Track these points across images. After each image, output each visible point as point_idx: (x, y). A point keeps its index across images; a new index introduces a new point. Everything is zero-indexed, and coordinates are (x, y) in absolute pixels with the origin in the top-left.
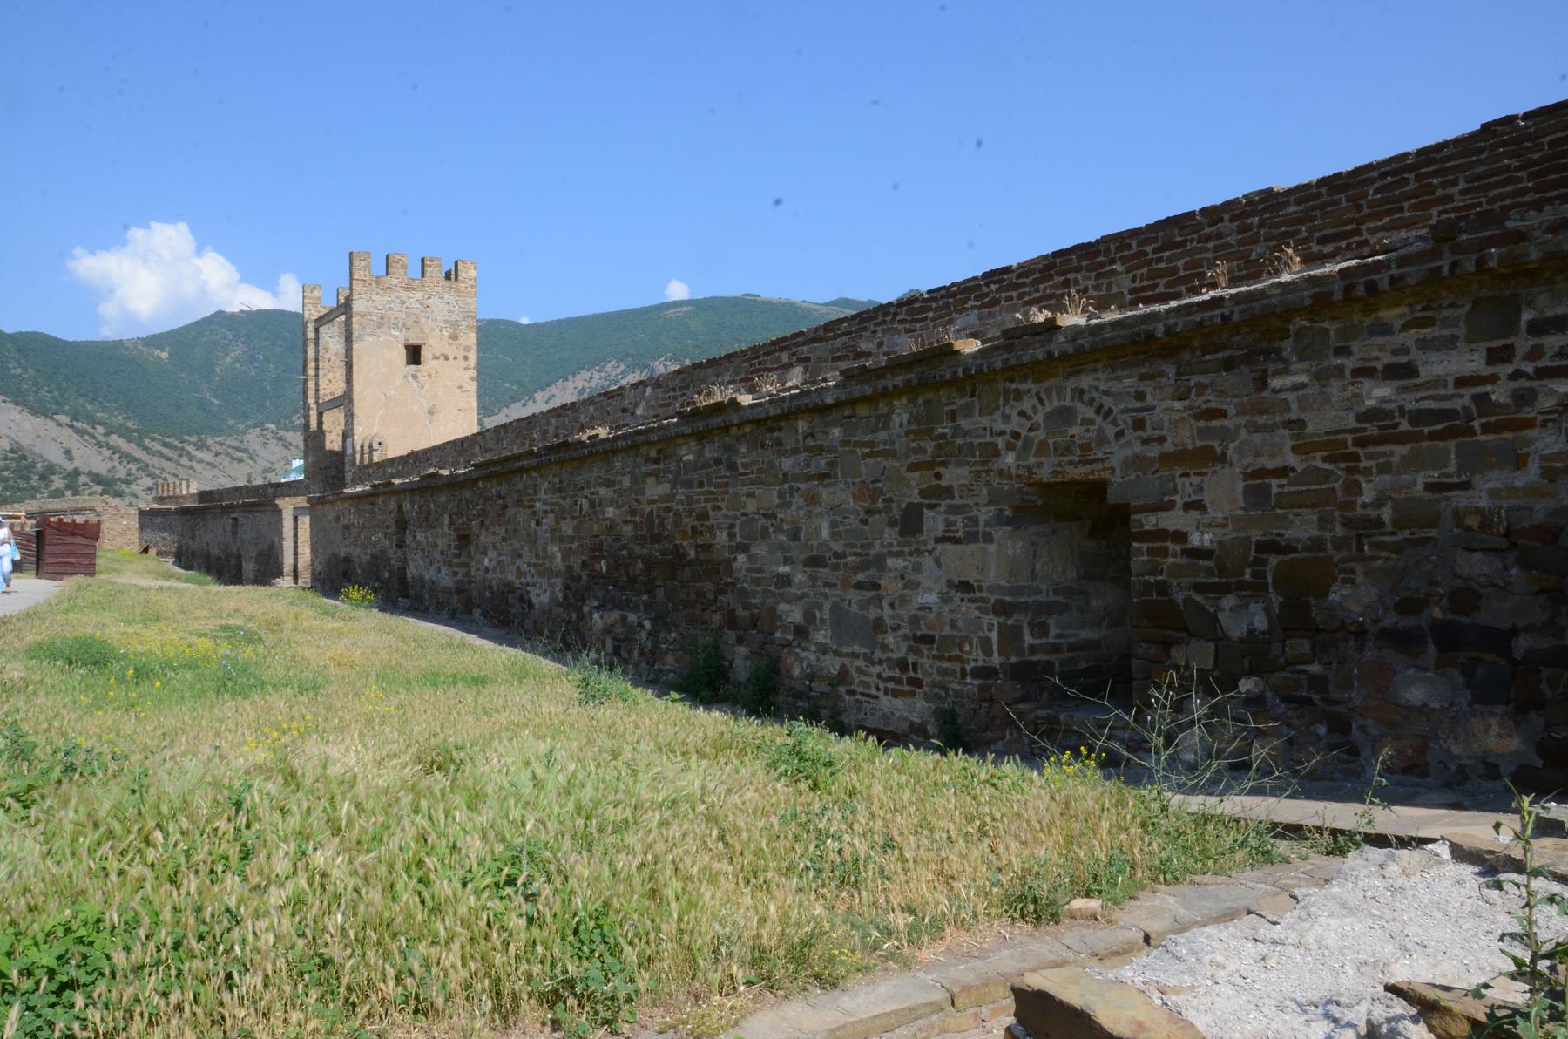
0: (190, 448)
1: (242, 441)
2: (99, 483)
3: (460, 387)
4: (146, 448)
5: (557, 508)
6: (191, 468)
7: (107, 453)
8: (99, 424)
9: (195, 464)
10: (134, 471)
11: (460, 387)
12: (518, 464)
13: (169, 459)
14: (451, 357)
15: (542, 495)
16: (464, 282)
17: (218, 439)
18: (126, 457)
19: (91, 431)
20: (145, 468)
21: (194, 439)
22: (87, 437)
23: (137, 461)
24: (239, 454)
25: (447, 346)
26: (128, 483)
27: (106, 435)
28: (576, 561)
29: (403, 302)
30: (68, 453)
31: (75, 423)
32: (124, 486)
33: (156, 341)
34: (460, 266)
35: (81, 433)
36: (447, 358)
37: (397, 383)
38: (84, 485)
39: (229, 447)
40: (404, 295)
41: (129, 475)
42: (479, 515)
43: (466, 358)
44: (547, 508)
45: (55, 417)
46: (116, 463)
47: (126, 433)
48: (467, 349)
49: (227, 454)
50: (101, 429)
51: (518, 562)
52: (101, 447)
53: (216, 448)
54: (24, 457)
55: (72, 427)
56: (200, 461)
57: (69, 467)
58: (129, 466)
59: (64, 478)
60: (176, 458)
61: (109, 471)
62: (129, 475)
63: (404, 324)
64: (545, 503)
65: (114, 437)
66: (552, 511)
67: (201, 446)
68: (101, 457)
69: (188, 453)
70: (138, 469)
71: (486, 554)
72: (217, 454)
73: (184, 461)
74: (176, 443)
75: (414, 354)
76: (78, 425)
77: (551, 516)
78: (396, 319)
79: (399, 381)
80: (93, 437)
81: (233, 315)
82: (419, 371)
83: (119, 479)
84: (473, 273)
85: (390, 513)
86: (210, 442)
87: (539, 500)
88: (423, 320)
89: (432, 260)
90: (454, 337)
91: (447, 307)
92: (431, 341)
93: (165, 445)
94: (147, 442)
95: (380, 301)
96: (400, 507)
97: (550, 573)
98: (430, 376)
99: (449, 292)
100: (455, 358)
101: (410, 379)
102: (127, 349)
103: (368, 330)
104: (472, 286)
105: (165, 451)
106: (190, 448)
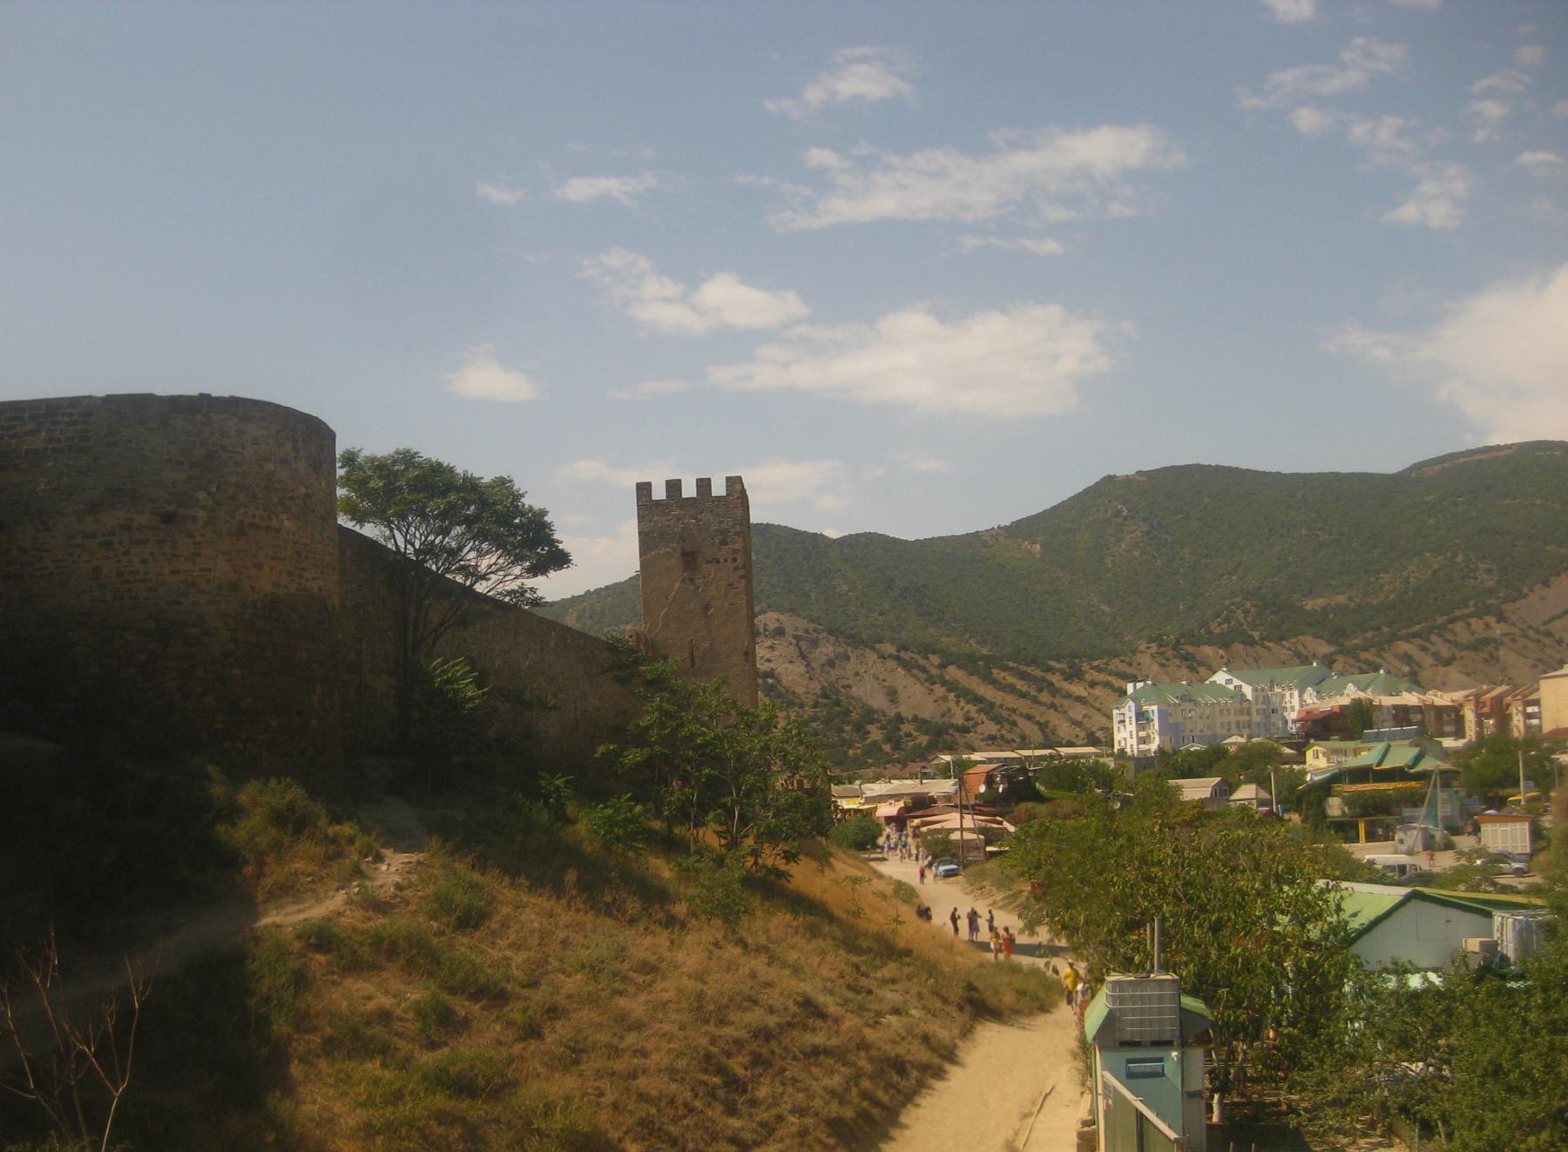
4: (994, 682)
7: (940, 690)
8: (934, 652)
9: (1057, 701)
10: (974, 714)
17: (1096, 663)
19: (922, 662)
20: (988, 708)
22: (915, 671)
23: (978, 700)
26: (965, 730)
27: (943, 666)
30: (892, 694)
31: (902, 654)
32: (957, 735)
33: (1023, 529)
35: (907, 666)
36: (718, 562)
38: (908, 735)
41: (968, 719)
43: (735, 560)
45: (878, 646)
46: (952, 704)
47: (969, 663)
48: (736, 551)
49: (1107, 685)
50: (935, 660)
52: (934, 683)
53: (1092, 675)
54: (838, 703)
55: (898, 658)
56: (1069, 696)
57: (892, 711)
59: (881, 728)
60: (1033, 693)
61: (943, 716)
62: (968, 719)
67: (1074, 675)
68: (933, 698)
69: (1051, 684)
70: (979, 711)
72: (1093, 684)
73: (1045, 697)
74: (1038, 673)
80: (924, 670)
81: (1127, 481)
86: (1085, 666)
93: (1023, 676)
101: (687, 581)
102: (985, 545)
105: (1020, 685)
106: (1056, 679)
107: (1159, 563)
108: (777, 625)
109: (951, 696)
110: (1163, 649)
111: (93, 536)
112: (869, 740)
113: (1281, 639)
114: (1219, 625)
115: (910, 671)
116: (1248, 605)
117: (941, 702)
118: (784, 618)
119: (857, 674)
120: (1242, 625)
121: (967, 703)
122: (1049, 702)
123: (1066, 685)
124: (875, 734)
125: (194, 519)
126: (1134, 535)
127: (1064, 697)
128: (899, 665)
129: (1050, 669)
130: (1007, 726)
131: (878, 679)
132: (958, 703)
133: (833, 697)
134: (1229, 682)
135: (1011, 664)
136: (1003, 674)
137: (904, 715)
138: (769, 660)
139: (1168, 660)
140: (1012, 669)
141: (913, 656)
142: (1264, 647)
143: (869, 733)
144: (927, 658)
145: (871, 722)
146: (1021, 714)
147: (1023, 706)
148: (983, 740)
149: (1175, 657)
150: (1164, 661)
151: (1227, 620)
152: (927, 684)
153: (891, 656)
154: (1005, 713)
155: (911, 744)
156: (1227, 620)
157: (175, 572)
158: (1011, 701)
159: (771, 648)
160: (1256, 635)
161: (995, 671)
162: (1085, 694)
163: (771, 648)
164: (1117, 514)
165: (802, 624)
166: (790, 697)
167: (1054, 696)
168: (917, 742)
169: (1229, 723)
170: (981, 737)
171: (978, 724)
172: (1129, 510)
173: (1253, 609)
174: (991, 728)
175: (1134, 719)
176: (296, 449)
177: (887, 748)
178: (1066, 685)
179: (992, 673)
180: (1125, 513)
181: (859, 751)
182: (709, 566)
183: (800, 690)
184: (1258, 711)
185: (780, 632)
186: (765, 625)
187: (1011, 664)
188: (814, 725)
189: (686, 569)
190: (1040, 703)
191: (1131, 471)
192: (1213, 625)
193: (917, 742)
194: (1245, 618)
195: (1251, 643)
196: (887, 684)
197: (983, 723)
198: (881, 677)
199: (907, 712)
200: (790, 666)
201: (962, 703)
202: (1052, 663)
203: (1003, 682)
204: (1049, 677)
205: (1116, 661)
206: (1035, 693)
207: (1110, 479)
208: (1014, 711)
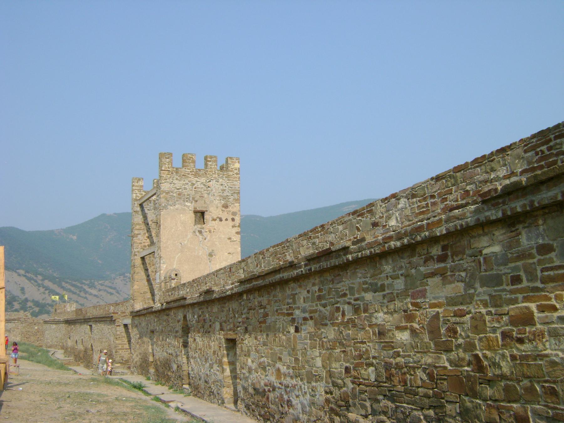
1: (113, 283)
2: (37, 306)
3: (230, 239)
4: (63, 287)
5: (316, 315)
6: (86, 298)
7: (42, 290)
8: (40, 274)
9: (87, 296)
11: (230, 239)
12: (278, 277)
14: (224, 219)
15: (301, 303)
16: (231, 171)
17: (100, 282)
19: (35, 278)
21: (87, 282)
22: (33, 282)
24: (111, 291)
25: (221, 213)
27: (43, 280)
28: (337, 367)
29: (193, 184)
31: (27, 274)
32: (50, 308)
33: (71, 230)
34: (229, 162)
35: (29, 279)
36: (221, 220)
37: (189, 236)
39: (106, 286)
40: (194, 180)
42: (243, 323)
43: (233, 220)
44: (307, 315)
45: (17, 271)
48: (234, 214)
49: (105, 290)
50: (40, 277)
51: (279, 365)
53: (99, 287)
55: (25, 276)
56: (91, 294)
57: (23, 297)
59: (19, 304)
60: (78, 293)
61: (43, 300)
63: (193, 199)
64: (304, 311)
66: (311, 318)
67: (92, 286)
69: (84, 290)
71: (249, 356)
72: (100, 290)
73: (82, 294)
74: (79, 284)
75: (201, 215)
76: (29, 275)
77: (311, 322)
78: (188, 195)
79: (190, 235)
80: (36, 281)
82: (203, 228)
83: (48, 304)
84: (237, 165)
85: (179, 321)
86: (96, 283)
87: (298, 308)
88: (206, 196)
89: (211, 157)
91: (221, 187)
92: (211, 209)
95: (178, 184)
96: (185, 317)
97: (311, 377)
98: (210, 231)
99: (222, 178)
100: (226, 220)
101: (198, 234)
103: (170, 203)
104: (237, 174)
105: (72, 289)
106: (86, 287)
109: (47, 292)
110: (125, 278)
115: (30, 281)
117: (42, 294)
123: (90, 290)
129: (82, 283)
131: (17, 284)
136: (66, 285)
137: (29, 299)
139: (127, 282)
140: (69, 283)
141: (31, 275)
143: (14, 305)
144: (37, 277)
145: (15, 301)
153: (23, 275)
161: (63, 283)
162: (97, 294)
168: (34, 310)
178: (90, 290)
182: (213, 222)
189: (196, 223)
190: (81, 297)
193: (34, 310)
196: (21, 286)
198: (18, 283)
199: (30, 298)
202: (84, 281)
205: (107, 282)
207: (103, 215)
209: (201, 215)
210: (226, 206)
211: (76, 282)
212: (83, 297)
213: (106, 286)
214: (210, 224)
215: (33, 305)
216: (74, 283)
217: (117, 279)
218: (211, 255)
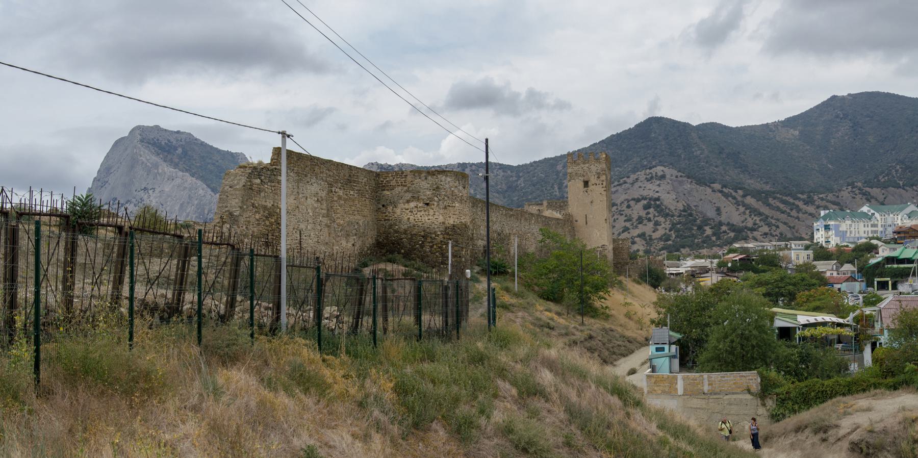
0: (800, 204)
1: (838, 197)
2: (733, 231)
4: (769, 205)
6: (798, 218)
7: (742, 209)
8: (740, 189)
9: (800, 215)
10: (758, 222)
13: (783, 212)
17: (821, 196)
18: (754, 212)
19: (734, 194)
20: (765, 219)
21: (805, 196)
22: (730, 199)
23: (760, 214)
27: (744, 196)
31: (724, 190)
32: (749, 232)
33: (790, 122)
35: (726, 196)
38: (725, 232)
39: (828, 201)
40: (583, 166)
41: (755, 224)
43: (602, 184)
45: (712, 185)
46: (747, 216)
47: (757, 194)
48: (603, 181)
50: (740, 192)
52: (739, 205)
54: (691, 215)
55: (721, 192)
57: (717, 219)
58: (755, 218)
59: (711, 228)
60: (788, 211)
62: (755, 224)
65: (749, 198)
68: (738, 213)
69: (798, 206)
73: (794, 213)
74: (792, 200)
79: (582, 193)
80: (734, 198)
81: (843, 98)
86: (816, 198)
90: (598, 178)
94: (771, 200)
95: (576, 168)
105: (782, 206)
106: (800, 204)
107: (857, 143)
108: (662, 173)
109: (748, 212)
110: (854, 190)
111: (408, 209)
112: (705, 235)
113: (912, 185)
114: (884, 177)
115: (727, 198)
116: (898, 167)
117: (742, 215)
118: (666, 169)
119: (701, 200)
120: (894, 177)
121: (755, 216)
122: (795, 216)
124: (708, 231)
125: (434, 204)
126: (845, 128)
127: (804, 213)
128: (722, 195)
130: (774, 228)
132: (750, 216)
133: (689, 211)
134: (869, 211)
135: (778, 195)
137: (723, 221)
138: (657, 192)
140: (779, 198)
141: (730, 190)
142: (904, 189)
143: (706, 230)
144: (736, 192)
146: (782, 222)
147: (783, 217)
148: (761, 235)
149: (860, 193)
150: (854, 196)
151: (887, 175)
152: (736, 205)
154: (773, 221)
155: (725, 237)
156: (887, 175)
157: (429, 219)
158: (778, 215)
159: (659, 185)
160: (901, 183)
161: (770, 199)
163: (659, 185)
164: (837, 117)
165: (675, 172)
166: (667, 211)
167: (798, 213)
168: (729, 235)
169: (868, 231)
170: (760, 233)
171: (760, 227)
172: (844, 115)
173: (900, 170)
174: (765, 229)
175: (823, 229)
176: (459, 183)
177: (714, 238)
179: (768, 200)
180: (841, 116)
181: (700, 240)
183: (673, 208)
184: (882, 225)
185: (663, 177)
186: (656, 173)
187: (778, 195)
188: (679, 226)
189: (585, 187)
190: (791, 216)
191: (845, 94)
192: (881, 177)
193: (729, 235)
194: (896, 174)
195: (898, 187)
196: (716, 205)
197: (762, 226)
198: (714, 201)
200: (668, 195)
201: (753, 216)
202: (799, 195)
203: (774, 205)
204: (797, 202)
206: (790, 211)
208: (778, 220)
209: (586, 184)
210: (598, 178)
211: (789, 198)
212: (794, 217)
213: (828, 201)
214: (591, 187)
215: (728, 230)
216: (784, 198)
217: (844, 191)
218: (592, 202)
